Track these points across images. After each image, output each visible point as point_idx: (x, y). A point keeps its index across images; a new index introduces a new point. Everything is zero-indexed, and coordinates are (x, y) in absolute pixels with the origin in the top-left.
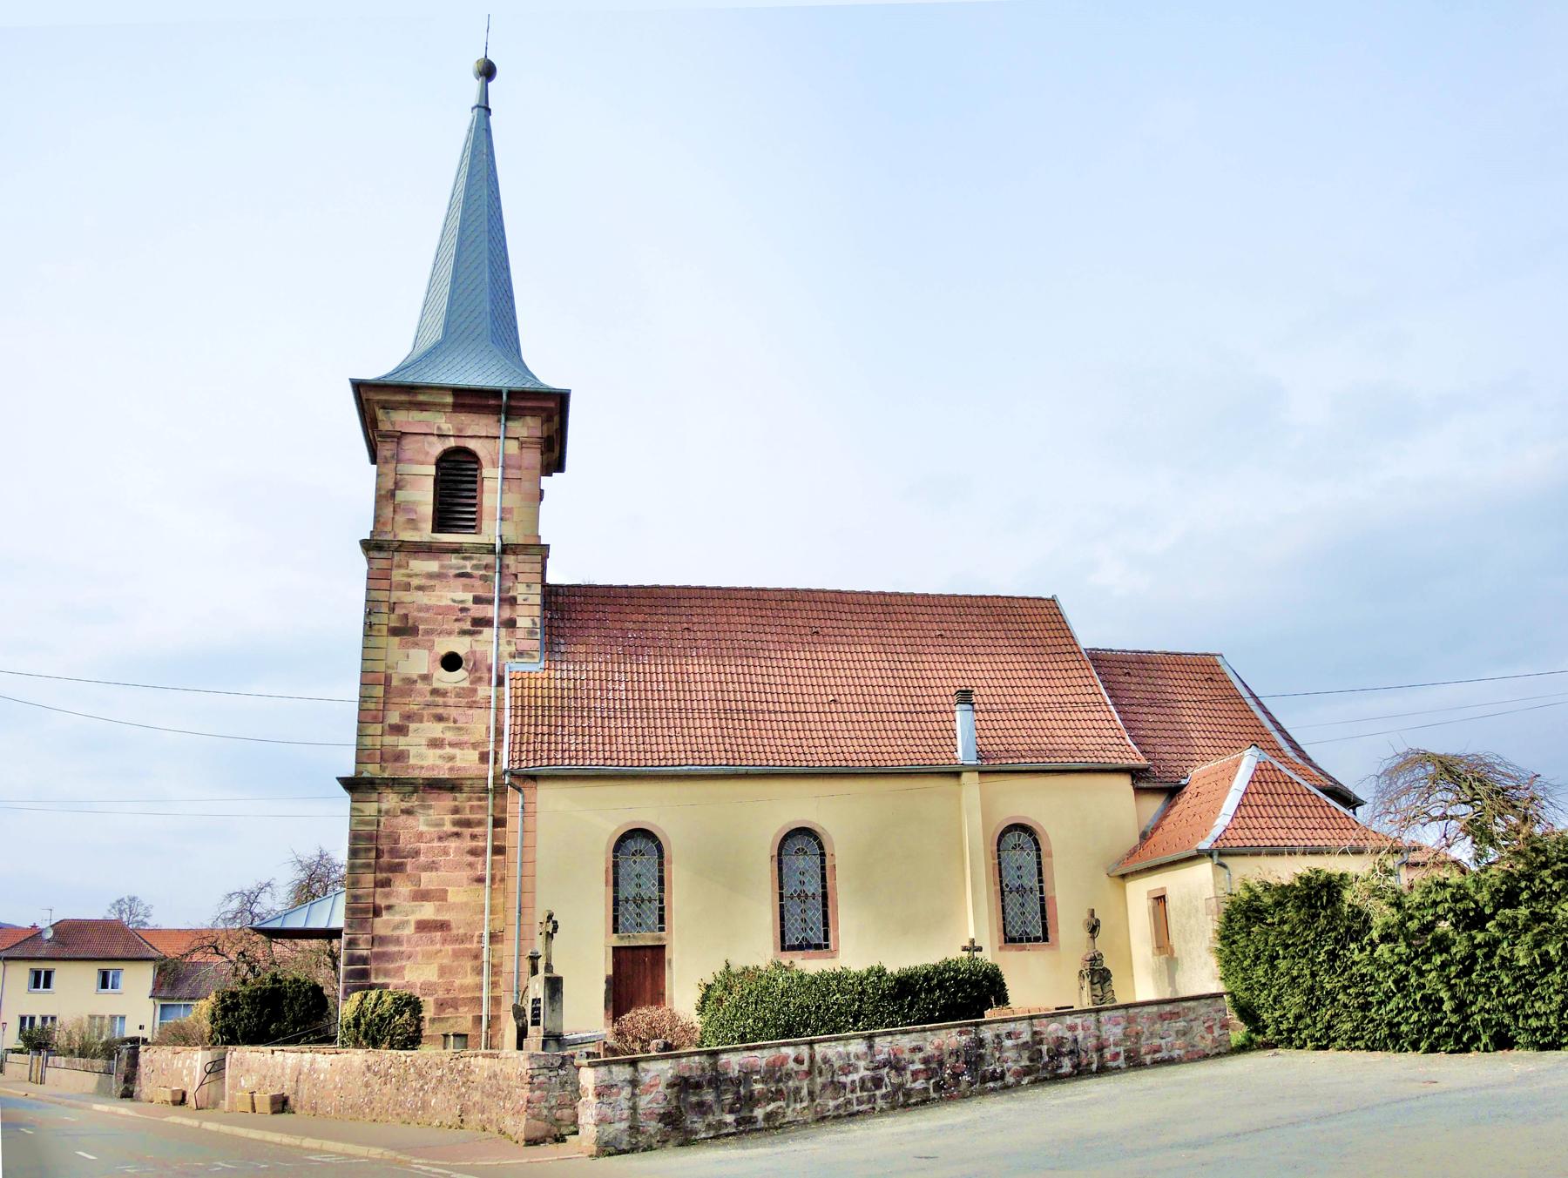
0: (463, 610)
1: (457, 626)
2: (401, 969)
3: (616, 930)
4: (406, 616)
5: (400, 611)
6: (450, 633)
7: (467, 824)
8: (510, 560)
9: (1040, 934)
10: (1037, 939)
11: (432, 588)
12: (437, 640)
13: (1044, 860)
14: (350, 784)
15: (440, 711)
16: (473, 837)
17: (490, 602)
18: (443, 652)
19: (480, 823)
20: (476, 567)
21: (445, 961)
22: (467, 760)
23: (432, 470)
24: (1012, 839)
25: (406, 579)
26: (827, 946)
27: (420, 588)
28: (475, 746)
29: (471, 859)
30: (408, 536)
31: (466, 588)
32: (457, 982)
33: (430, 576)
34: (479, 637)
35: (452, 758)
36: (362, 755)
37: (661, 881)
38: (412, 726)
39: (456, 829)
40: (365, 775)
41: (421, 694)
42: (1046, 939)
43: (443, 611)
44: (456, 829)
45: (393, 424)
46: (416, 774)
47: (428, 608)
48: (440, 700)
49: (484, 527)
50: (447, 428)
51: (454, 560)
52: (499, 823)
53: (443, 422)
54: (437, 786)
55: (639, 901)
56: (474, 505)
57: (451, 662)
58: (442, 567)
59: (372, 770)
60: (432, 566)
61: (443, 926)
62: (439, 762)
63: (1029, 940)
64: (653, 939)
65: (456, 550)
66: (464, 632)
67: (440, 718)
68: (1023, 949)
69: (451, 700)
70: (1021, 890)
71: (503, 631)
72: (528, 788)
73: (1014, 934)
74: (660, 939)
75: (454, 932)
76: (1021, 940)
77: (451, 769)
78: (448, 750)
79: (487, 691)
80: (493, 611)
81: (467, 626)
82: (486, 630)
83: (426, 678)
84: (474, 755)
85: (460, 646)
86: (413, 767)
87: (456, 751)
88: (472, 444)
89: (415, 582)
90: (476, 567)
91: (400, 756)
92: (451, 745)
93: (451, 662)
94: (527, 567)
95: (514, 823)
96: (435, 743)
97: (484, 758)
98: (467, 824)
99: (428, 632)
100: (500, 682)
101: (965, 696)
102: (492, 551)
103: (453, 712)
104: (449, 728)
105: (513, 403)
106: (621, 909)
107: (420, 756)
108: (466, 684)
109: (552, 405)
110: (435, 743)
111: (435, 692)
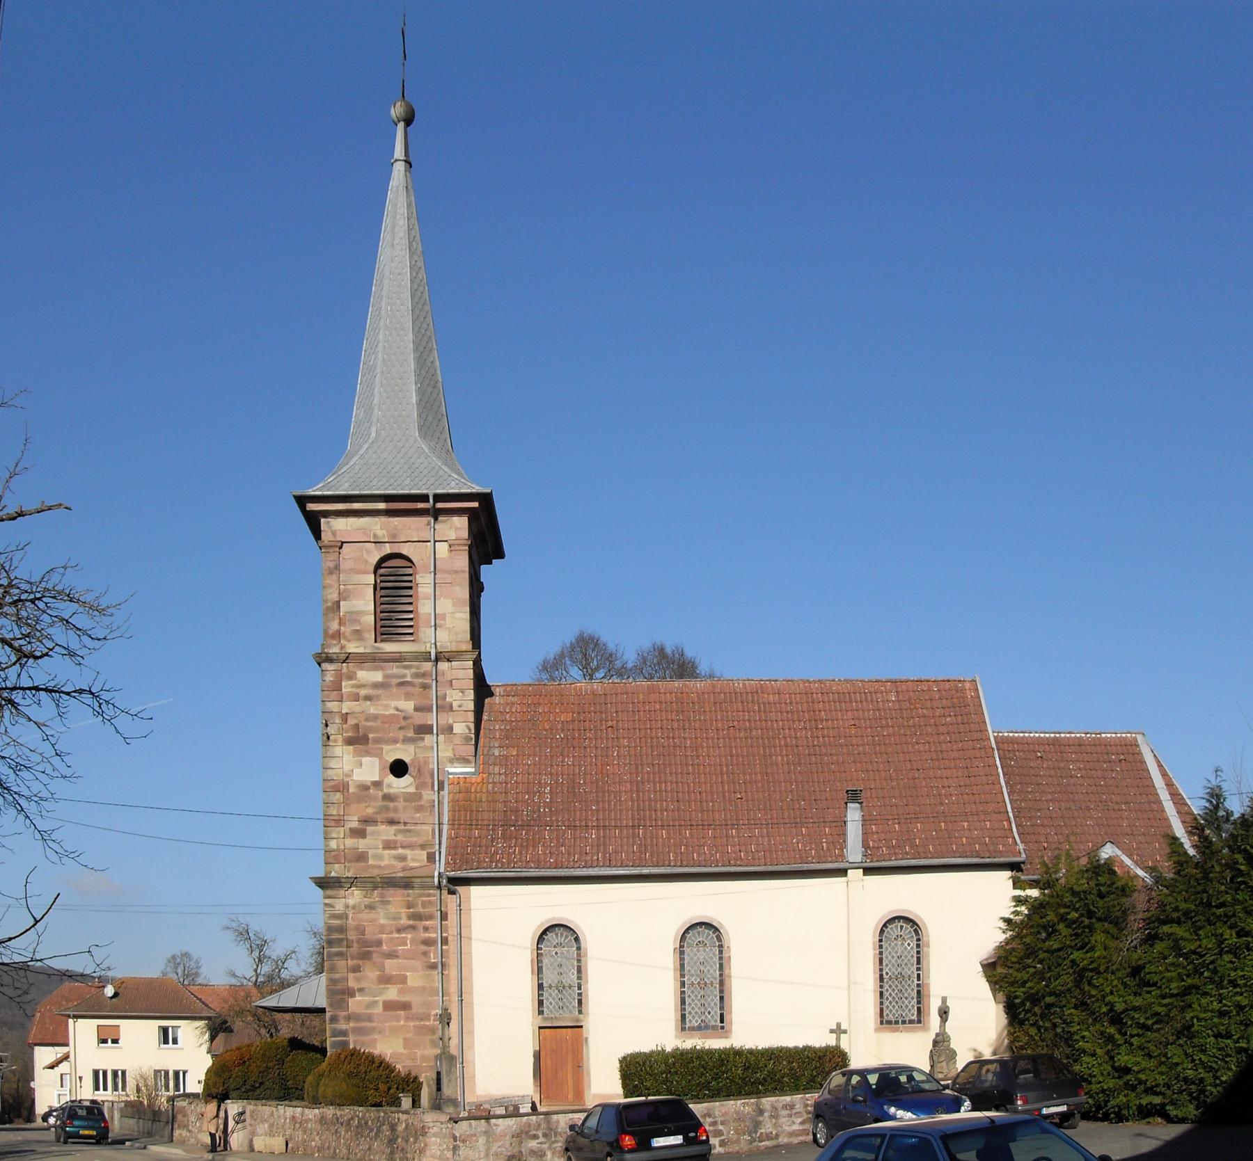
0: (405, 718)
1: (401, 735)
2: (375, 1041)
3: (541, 1012)
4: (357, 726)
5: (351, 721)
6: (395, 741)
7: (418, 917)
8: (443, 666)
9: (915, 1017)
10: (911, 1022)
11: (378, 698)
12: (386, 748)
13: (725, 955)
14: (324, 883)
15: (392, 815)
16: (426, 929)
17: (429, 710)
18: (391, 760)
19: (430, 917)
20: (416, 675)
21: (408, 1036)
22: (416, 859)
23: (371, 579)
24: (894, 930)
25: (354, 690)
26: (722, 1028)
27: (368, 698)
28: (423, 847)
29: (424, 948)
30: (353, 648)
31: (408, 697)
32: (419, 1053)
33: (376, 686)
34: (421, 744)
35: (403, 858)
36: (331, 857)
37: (579, 970)
38: (369, 829)
39: (411, 922)
40: (333, 874)
41: (374, 798)
42: (919, 1022)
43: (390, 719)
44: (411, 922)
45: (334, 533)
46: (375, 872)
47: (375, 717)
48: (392, 805)
49: (421, 635)
50: (382, 534)
51: (394, 669)
52: (444, 917)
53: (377, 526)
54: (390, 883)
55: (561, 988)
56: (411, 588)
57: (399, 769)
58: (386, 676)
59: (336, 871)
60: (377, 676)
61: (406, 1006)
62: (394, 863)
63: (904, 1022)
64: (572, 1020)
65: (398, 659)
66: (406, 740)
67: (392, 822)
68: (897, 1030)
69: (400, 804)
70: (900, 977)
71: (441, 737)
72: (461, 889)
73: (891, 1017)
74: (578, 1020)
75: (414, 1010)
76: (897, 1022)
77: (404, 870)
78: (401, 851)
79: (429, 795)
80: (431, 718)
81: (411, 734)
82: (427, 737)
83: (377, 784)
84: (423, 855)
85: (405, 753)
86: (373, 867)
87: (407, 852)
88: (405, 550)
89: (363, 692)
90: (416, 675)
91: (361, 857)
92: (402, 847)
93: (399, 769)
94: (461, 674)
95: (453, 918)
96: (388, 845)
97: (431, 858)
98: (418, 917)
99: (378, 741)
100: (441, 787)
101: (854, 796)
102: (429, 660)
103: (403, 817)
104: (400, 831)
105: (439, 505)
106: (546, 994)
107: (380, 857)
108: (412, 790)
109: (476, 504)
110: (388, 845)
111: (387, 797)
